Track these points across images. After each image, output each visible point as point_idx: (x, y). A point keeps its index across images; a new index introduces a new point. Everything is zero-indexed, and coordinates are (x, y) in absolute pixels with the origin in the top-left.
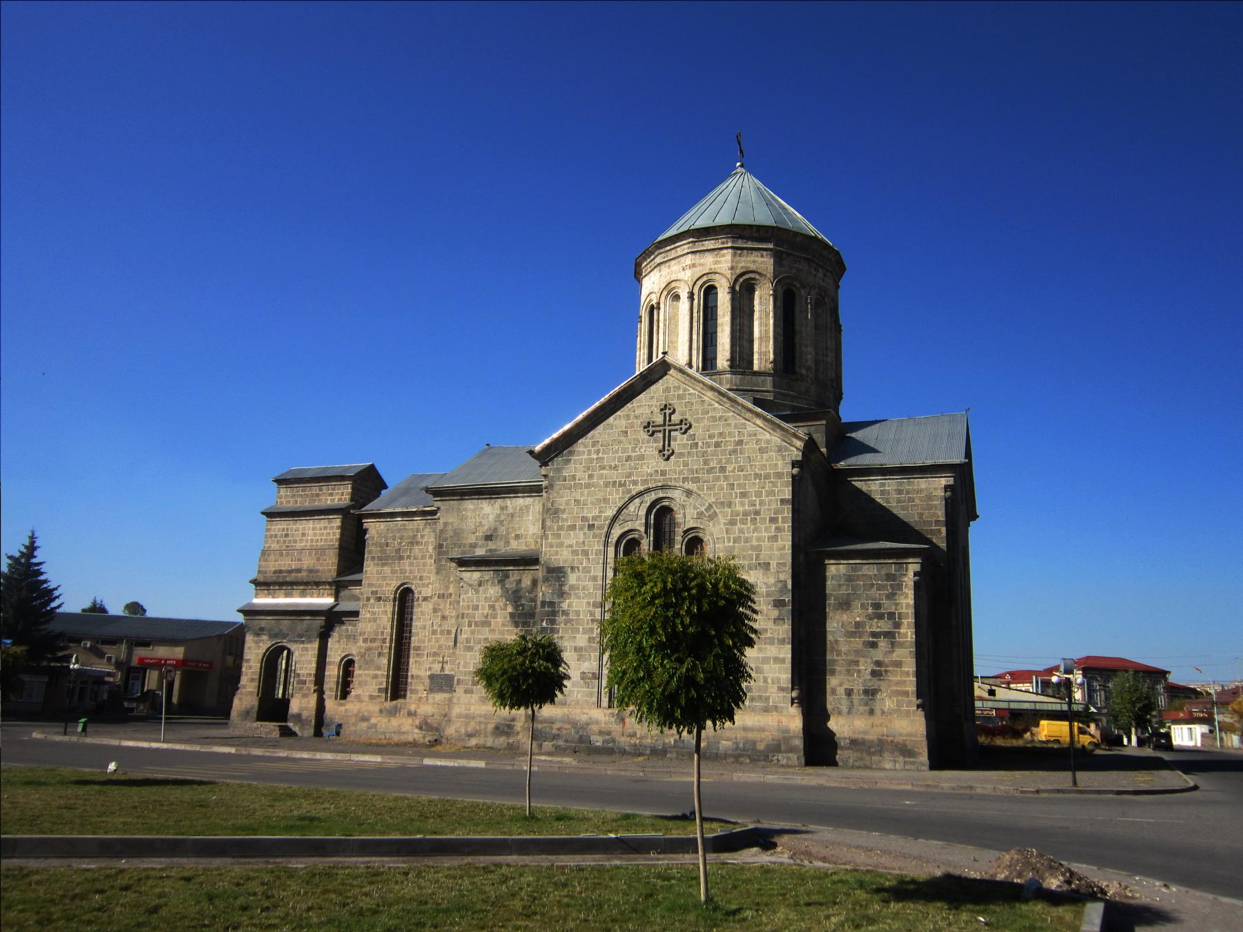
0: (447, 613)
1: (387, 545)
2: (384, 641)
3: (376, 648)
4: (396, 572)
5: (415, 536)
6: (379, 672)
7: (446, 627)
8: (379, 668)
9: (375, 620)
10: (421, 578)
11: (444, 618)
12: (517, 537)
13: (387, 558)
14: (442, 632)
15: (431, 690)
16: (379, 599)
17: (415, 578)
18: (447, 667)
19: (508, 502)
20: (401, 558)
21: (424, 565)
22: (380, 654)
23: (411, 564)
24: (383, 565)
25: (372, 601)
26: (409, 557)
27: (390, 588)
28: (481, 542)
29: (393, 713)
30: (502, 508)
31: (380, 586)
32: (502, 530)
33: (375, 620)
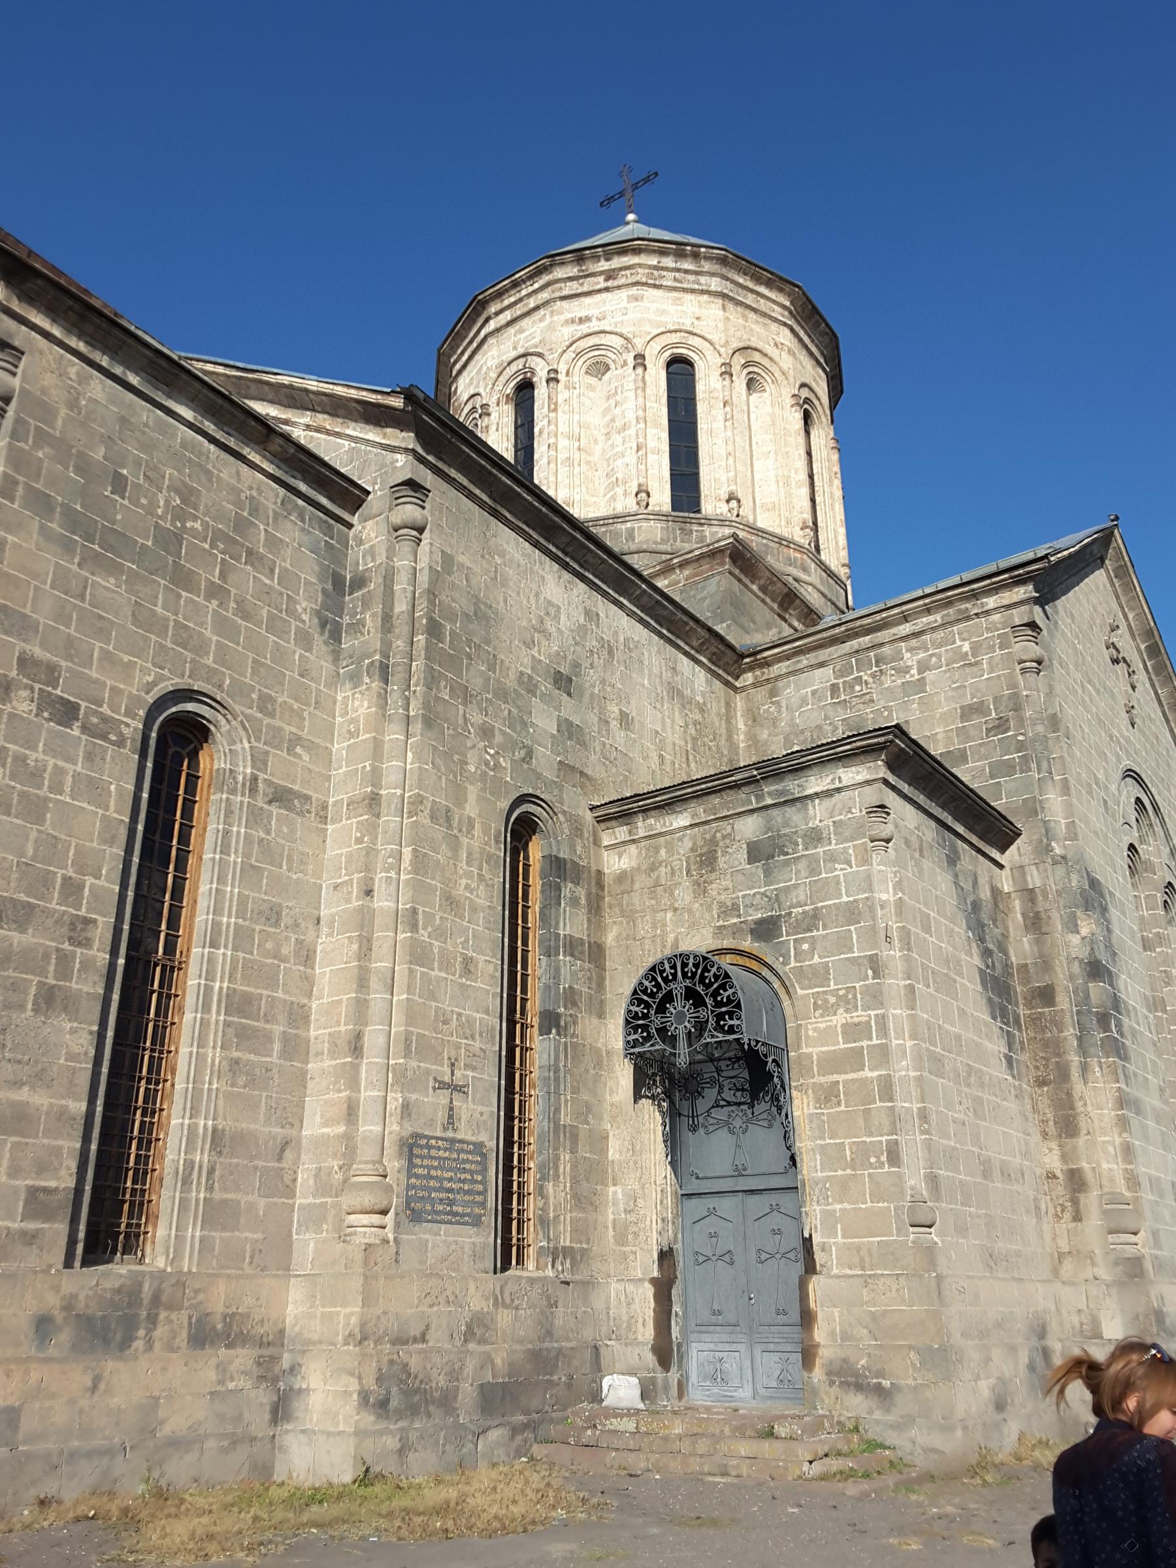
0: (460, 891)
1: (120, 484)
2: (78, 931)
3: (29, 960)
4: (156, 625)
5: (241, 525)
6: (39, 1099)
7: (455, 945)
8: (40, 1079)
9: (35, 810)
10: (266, 704)
11: (451, 902)
12: (625, 720)
13: (116, 542)
14: (446, 966)
15: (414, 1214)
16: (67, 712)
17: (240, 690)
18: (466, 1108)
19: (602, 606)
20: (182, 579)
21: (280, 655)
22: (48, 1000)
23: (223, 626)
24: (92, 560)
25: (22, 704)
26: (214, 591)
27: (128, 689)
28: (546, 686)
29: (110, 1331)
30: (587, 613)
31: (69, 647)
32: (591, 677)
33: (35, 810)
